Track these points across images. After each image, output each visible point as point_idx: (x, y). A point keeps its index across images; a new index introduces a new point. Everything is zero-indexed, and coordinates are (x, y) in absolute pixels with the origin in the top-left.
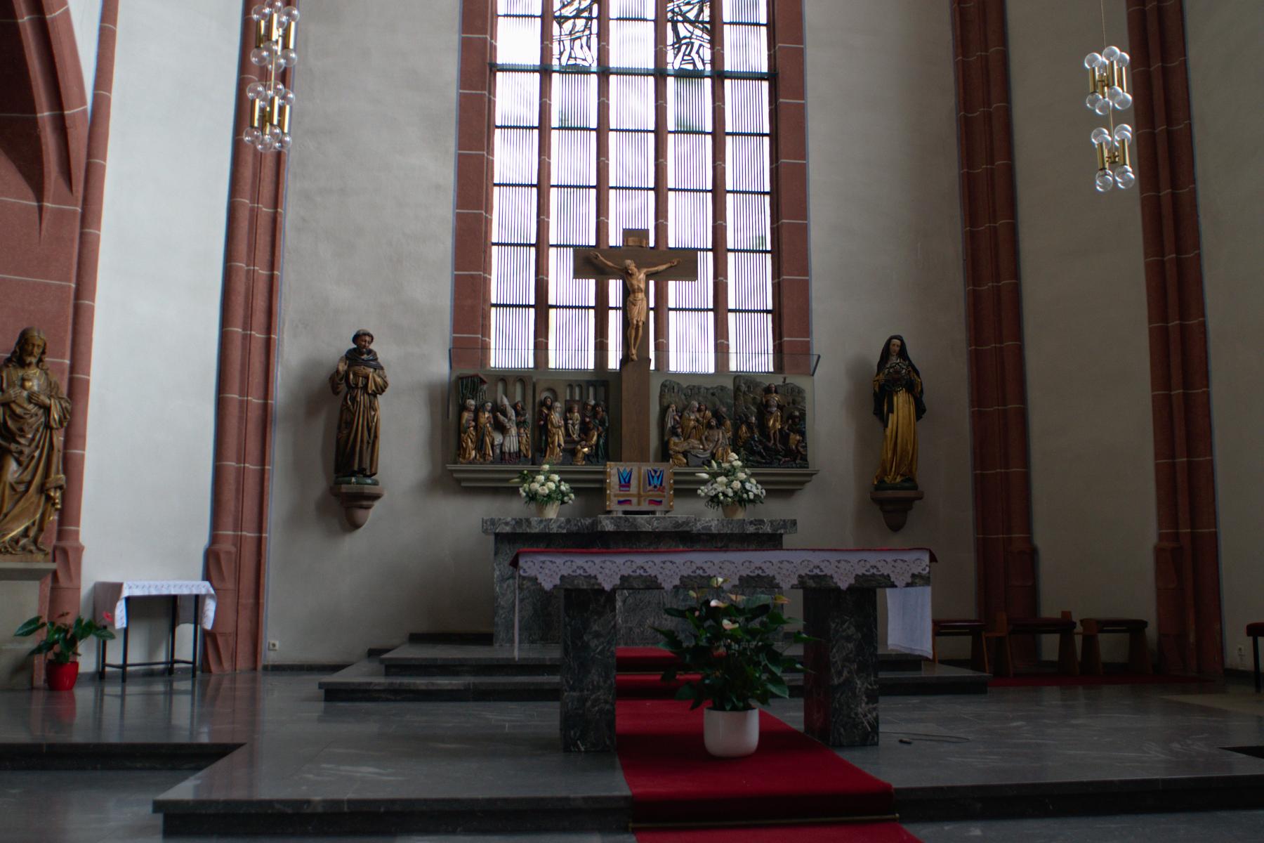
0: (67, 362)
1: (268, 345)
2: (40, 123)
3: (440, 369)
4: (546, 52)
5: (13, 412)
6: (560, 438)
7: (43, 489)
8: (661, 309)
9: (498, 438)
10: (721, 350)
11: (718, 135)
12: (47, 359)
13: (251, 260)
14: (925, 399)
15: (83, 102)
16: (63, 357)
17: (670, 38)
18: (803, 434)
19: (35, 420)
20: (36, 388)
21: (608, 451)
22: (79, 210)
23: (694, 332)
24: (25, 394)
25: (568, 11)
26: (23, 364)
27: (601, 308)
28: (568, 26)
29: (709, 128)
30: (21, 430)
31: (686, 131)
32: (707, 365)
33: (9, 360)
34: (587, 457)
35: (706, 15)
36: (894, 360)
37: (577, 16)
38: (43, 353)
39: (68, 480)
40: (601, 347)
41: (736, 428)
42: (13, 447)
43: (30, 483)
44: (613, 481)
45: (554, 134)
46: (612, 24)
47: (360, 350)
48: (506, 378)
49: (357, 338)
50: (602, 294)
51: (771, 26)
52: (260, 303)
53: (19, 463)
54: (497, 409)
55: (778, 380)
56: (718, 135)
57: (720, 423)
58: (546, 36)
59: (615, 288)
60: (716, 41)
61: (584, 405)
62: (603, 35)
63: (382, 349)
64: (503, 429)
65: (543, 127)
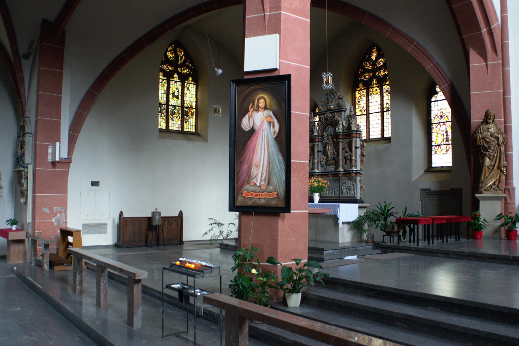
0: (503, 120)
2: (483, 34)
5: (486, 141)
7: (499, 168)
12: (495, 120)
15: (497, 21)
16: (501, 118)
19: (494, 143)
20: (493, 131)
22: (501, 62)
24: (489, 134)
30: (489, 147)
33: (482, 122)
38: (494, 118)
39: (508, 164)
42: (487, 153)
43: (494, 166)
53: (490, 159)
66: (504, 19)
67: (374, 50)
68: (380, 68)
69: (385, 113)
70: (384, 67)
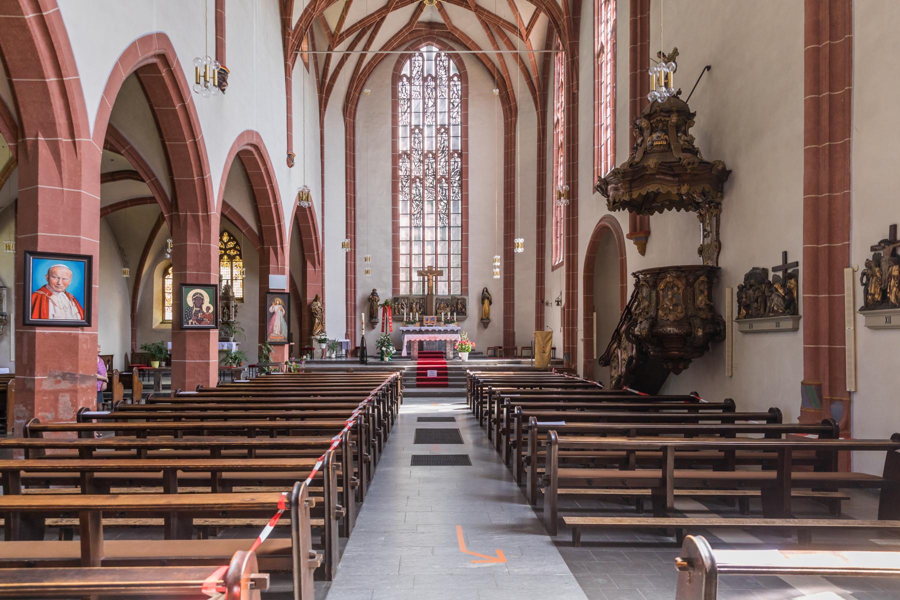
4: (411, 223)
8: (436, 281)
9: (402, 310)
10: (449, 291)
11: (449, 241)
13: (351, 274)
17: (439, 218)
18: (465, 309)
21: (424, 313)
23: (443, 287)
25: (416, 213)
26: (316, 301)
27: (424, 281)
28: (416, 216)
35: (447, 212)
40: (424, 291)
44: (425, 320)
48: (404, 298)
49: (373, 290)
50: (424, 279)
51: (462, 214)
52: (353, 283)
54: (402, 304)
55: (460, 297)
56: (449, 241)
57: (448, 307)
58: (411, 219)
59: (426, 277)
60: (449, 218)
61: (420, 303)
62: (423, 218)
64: (403, 309)
66: (323, 247)
67: (226, 234)
68: (230, 249)
70: (234, 248)
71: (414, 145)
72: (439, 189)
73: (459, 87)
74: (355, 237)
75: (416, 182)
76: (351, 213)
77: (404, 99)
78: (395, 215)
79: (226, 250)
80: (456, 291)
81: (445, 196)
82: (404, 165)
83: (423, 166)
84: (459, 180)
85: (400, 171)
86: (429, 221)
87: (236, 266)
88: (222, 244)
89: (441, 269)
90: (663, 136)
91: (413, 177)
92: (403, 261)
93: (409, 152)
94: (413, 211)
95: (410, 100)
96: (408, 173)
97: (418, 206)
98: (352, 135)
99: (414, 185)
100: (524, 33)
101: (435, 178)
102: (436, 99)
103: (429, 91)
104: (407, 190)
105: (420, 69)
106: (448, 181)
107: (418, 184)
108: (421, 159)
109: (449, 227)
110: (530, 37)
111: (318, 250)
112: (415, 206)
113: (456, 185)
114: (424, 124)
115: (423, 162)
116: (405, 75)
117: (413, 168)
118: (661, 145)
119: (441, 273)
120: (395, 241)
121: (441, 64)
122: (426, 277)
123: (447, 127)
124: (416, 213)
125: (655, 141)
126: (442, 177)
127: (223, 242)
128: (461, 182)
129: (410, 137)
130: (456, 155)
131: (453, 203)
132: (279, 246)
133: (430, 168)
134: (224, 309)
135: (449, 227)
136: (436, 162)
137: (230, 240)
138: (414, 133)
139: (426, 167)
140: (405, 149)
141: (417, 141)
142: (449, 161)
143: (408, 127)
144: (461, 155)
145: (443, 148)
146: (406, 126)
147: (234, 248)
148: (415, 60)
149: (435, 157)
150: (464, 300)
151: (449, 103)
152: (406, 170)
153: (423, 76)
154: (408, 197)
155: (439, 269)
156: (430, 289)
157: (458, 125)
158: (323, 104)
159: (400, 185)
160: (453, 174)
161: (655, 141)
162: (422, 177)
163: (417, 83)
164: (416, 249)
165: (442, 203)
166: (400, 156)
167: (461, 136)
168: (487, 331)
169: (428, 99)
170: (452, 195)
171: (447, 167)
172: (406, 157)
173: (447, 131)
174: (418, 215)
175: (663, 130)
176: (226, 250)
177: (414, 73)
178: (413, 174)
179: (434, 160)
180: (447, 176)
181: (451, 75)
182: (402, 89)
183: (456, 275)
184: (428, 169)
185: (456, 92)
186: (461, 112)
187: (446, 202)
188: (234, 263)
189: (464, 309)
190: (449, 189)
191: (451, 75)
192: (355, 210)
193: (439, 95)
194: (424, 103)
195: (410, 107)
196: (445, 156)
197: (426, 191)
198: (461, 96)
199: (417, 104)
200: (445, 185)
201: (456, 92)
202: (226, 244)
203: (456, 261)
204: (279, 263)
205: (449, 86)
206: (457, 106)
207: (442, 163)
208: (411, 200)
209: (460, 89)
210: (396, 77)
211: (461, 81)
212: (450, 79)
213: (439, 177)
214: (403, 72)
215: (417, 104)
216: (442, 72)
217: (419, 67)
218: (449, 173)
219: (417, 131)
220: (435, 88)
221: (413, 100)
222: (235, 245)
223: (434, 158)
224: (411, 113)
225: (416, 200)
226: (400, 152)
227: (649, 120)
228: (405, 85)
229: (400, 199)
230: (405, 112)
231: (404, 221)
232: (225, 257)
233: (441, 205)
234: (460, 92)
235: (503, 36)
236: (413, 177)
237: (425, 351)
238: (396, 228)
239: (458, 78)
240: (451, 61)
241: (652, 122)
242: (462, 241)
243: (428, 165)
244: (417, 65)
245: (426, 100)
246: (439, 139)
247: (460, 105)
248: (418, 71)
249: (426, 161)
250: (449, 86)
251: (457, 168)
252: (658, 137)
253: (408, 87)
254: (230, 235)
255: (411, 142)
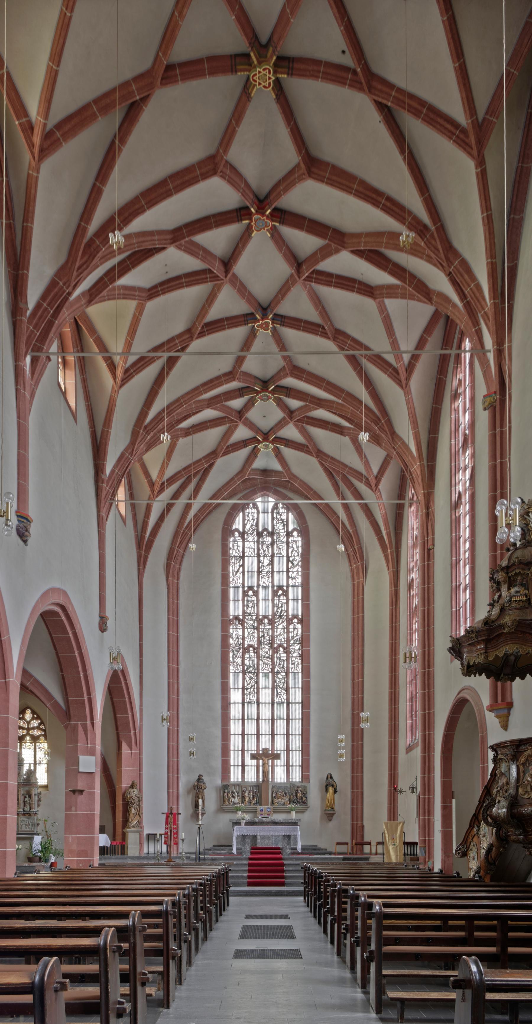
1: (178, 777)
3: (219, 782)
4: (243, 699)
6: (247, 799)
8: (273, 766)
9: (233, 799)
11: (288, 720)
13: (173, 757)
14: (338, 788)
18: (306, 798)
21: (259, 802)
28: (249, 690)
29: (285, 718)
31: (280, 718)
32: (284, 780)
34: (254, 804)
36: (329, 779)
37: (251, 688)
41: (290, 796)
45: (246, 721)
46: (260, 690)
47: (200, 779)
49: (199, 776)
52: (176, 768)
54: (233, 792)
55: (300, 785)
56: (288, 720)
58: (243, 694)
59: (261, 762)
63: (205, 778)
64: (233, 797)
65: (243, 719)
67: (28, 711)
68: (33, 728)
69: (37, 765)
70: (38, 728)
71: (247, 609)
72: (276, 659)
73: (299, 544)
74: (178, 714)
75: (249, 652)
76: (173, 686)
77: (236, 557)
78: (225, 689)
79: (28, 729)
80: (296, 776)
81: (283, 667)
82: (235, 631)
83: (258, 633)
84: (299, 649)
85: (231, 640)
86: (266, 696)
87: (39, 748)
88: (24, 723)
89: (279, 752)
90: (523, 591)
91: (246, 646)
92: (235, 742)
93: (241, 617)
94: (246, 685)
95: (242, 557)
96: (240, 641)
97: (251, 678)
98: (175, 596)
99: (247, 655)
100: (373, 482)
101: (272, 647)
102: (273, 556)
103: (265, 547)
104: (239, 660)
105: (255, 522)
106: (287, 651)
107: (252, 654)
108: (256, 625)
109: (288, 704)
110: (380, 487)
111: (135, 729)
112: (248, 679)
113: (295, 655)
114: (258, 586)
115: (257, 629)
116: (237, 530)
117: (246, 636)
118: (520, 601)
119: (277, 757)
120: (226, 719)
121: (278, 517)
122: (261, 762)
123: (285, 588)
124: (249, 686)
125: (514, 596)
126: (280, 646)
127: (25, 720)
128: (302, 652)
129: (243, 600)
130: (296, 620)
131: (293, 676)
132: (89, 722)
133: (266, 635)
134: (25, 797)
135: (288, 704)
136: (273, 629)
137: (33, 718)
138: (248, 595)
139: (261, 634)
140: (236, 614)
141: (250, 604)
142: (288, 628)
143: (241, 589)
144: (301, 621)
145: (281, 613)
146: (238, 587)
147: (38, 728)
148: (249, 513)
149: (272, 622)
150: (305, 788)
151: (288, 561)
152: (237, 638)
153: (258, 530)
154: (240, 669)
155: (276, 752)
156: (265, 774)
157: (298, 586)
158: (142, 561)
159: (231, 655)
160: (292, 642)
161: (514, 596)
162: (256, 646)
163: (250, 538)
164: (250, 728)
165: (279, 676)
166: (230, 622)
167: (302, 600)
168: (331, 824)
169: (264, 556)
170: (291, 666)
171: (285, 635)
172: (237, 623)
173: (286, 593)
174: (252, 690)
175: (522, 585)
176: (28, 729)
177: (248, 526)
178: (246, 642)
179: (270, 627)
180: (285, 645)
181: (290, 529)
182: (233, 545)
183: (296, 758)
184: (263, 636)
185: (296, 549)
186: (301, 572)
187: (284, 674)
188: (38, 744)
189: (304, 798)
190: (288, 660)
191: (290, 529)
192: (178, 684)
193: (276, 552)
194: (259, 561)
195: (243, 566)
196: (283, 622)
197: (261, 662)
198: (301, 554)
199: (250, 563)
200: (283, 655)
201: (296, 549)
202: (28, 723)
203: (296, 743)
204: (89, 742)
205: (288, 543)
206: (297, 564)
207: (279, 630)
208: (244, 672)
209: (300, 545)
210: (227, 532)
211: (301, 536)
212: (289, 534)
213: (275, 646)
214: (235, 527)
215: (250, 563)
216: (280, 527)
217: (254, 520)
218: (288, 641)
219: (250, 593)
220: (272, 544)
221: (246, 558)
222: (40, 724)
223: (269, 624)
224: (243, 572)
225: (249, 672)
226: (231, 617)
227: (507, 573)
228: (236, 541)
229: (231, 671)
230: (237, 572)
231: (235, 696)
232: (28, 738)
233: (278, 678)
234: (300, 549)
235: (350, 485)
236: (246, 646)
237: (259, 845)
238: (226, 704)
239: (298, 533)
240: (290, 514)
241: (510, 575)
242: (302, 719)
243: (263, 632)
244: (251, 518)
245: (262, 558)
246: (276, 602)
247: (300, 564)
248: (252, 525)
249: (261, 627)
250: (288, 543)
251: (297, 635)
252: (517, 592)
253: (240, 544)
254: (33, 712)
255: (243, 606)
